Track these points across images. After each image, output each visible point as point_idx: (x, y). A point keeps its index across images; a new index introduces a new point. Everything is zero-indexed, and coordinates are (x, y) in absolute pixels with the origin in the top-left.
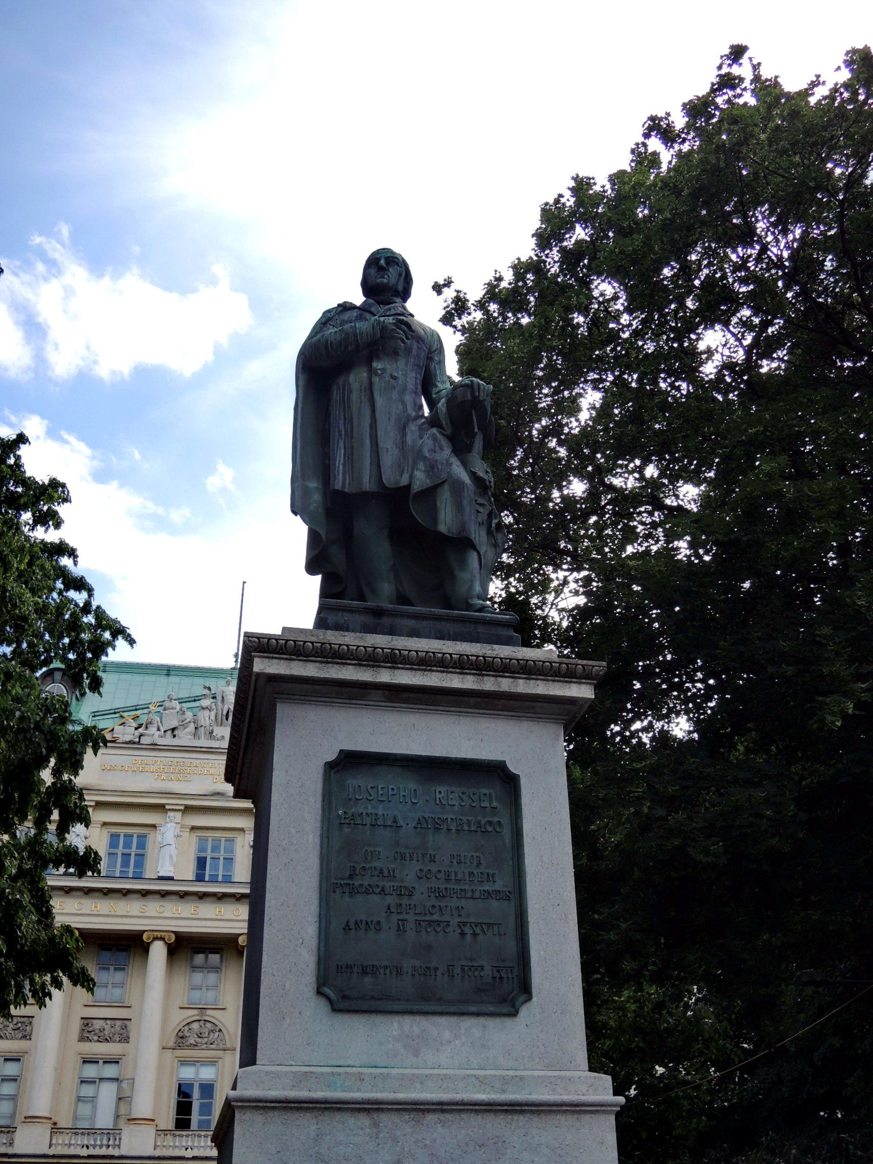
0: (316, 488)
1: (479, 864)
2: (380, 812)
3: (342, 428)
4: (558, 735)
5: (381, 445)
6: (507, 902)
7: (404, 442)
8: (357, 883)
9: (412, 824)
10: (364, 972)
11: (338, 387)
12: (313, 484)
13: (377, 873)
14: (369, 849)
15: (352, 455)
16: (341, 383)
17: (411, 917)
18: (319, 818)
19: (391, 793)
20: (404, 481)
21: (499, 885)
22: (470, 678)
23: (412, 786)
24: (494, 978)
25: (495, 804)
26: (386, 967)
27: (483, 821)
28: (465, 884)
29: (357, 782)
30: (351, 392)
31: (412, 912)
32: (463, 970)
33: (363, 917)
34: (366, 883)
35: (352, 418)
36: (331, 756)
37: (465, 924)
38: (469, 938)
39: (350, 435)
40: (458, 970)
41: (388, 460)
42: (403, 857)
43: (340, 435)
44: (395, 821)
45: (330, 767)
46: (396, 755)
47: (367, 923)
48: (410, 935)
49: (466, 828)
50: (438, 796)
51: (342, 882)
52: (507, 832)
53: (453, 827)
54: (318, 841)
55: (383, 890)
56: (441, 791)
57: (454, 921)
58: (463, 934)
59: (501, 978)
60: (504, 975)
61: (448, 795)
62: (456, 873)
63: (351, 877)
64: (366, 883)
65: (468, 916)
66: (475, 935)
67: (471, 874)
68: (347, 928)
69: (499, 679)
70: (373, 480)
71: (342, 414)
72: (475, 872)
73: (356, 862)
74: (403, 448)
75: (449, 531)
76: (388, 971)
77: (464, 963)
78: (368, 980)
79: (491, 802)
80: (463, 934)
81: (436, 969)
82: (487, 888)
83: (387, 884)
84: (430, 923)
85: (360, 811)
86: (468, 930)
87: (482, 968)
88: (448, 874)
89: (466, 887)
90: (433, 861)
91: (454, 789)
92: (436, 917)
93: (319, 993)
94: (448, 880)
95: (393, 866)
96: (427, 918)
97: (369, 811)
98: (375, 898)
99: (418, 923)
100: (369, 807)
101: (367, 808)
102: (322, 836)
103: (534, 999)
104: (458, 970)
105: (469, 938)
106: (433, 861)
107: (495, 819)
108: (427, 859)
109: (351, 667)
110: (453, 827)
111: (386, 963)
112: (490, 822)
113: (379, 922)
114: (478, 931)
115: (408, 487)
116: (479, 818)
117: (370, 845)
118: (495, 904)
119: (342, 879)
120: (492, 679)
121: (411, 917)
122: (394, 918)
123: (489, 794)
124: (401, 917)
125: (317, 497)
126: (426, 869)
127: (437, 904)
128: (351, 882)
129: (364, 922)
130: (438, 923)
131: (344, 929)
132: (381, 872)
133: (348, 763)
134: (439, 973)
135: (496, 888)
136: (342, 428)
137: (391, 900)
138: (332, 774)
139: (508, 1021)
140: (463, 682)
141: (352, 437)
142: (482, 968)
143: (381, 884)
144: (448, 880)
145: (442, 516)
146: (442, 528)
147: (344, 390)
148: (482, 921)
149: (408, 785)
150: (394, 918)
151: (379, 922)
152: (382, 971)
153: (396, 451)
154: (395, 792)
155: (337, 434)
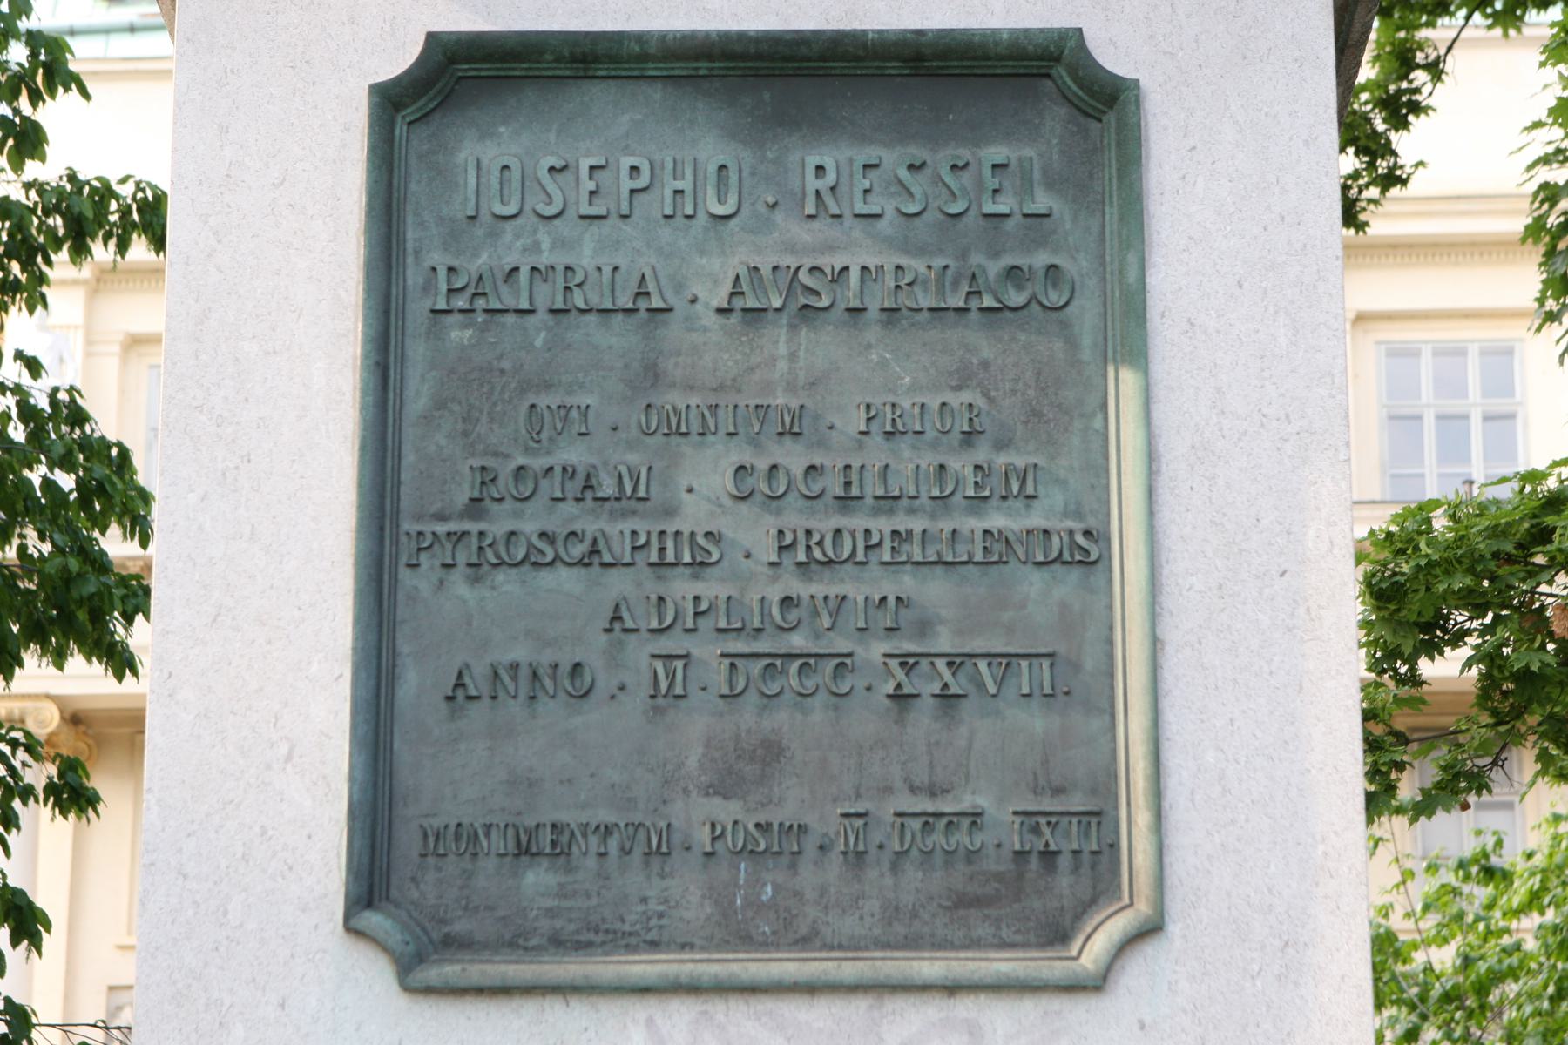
2: (585, 258)
6: (1075, 574)
8: (497, 529)
10: (524, 850)
13: (574, 487)
14: (543, 401)
17: (707, 650)
19: (627, 184)
23: (712, 150)
25: (1042, 201)
26: (607, 830)
27: (994, 268)
28: (911, 511)
29: (490, 152)
31: (705, 624)
33: (520, 653)
34: (530, 527)
37: (908, 663)
46: (640, 37)
47: (535, 675)
51: (441, 528)
55: (594, 551)
56: (823, 160)
63: (475, 508)
64: (530, 527)
68: (458, 694)
73: (496, 454)
76: (613, 844)
78: (537, 879)
82: (997, 520)
84: (775, 663)
85: (509, 261)
91: (871, 153)
93: (351, 929)
94: (846, 502)
95: (633, 458)
97: (544, 260)
98: (565, 579)
100: (546, 244)
101: (535, 247)
107: (1041, 259)
111: (605, 816)
112: (1013, 273)
116: (976, 259)
117: (548, 386)
118: (1033, 583)
119: (441, 517)
121: (707, 650)
123: (1010, 160)
124: (666, 645)
126: (763, 465)
128: (473, 527)
129: (524, 673)
131: (450, 699)
138: (400, 129)
142: (975, 818)
143: (590, 526)
148: (978, 645)
149: (698, 146)
150: (639, 652)
152: (594, 840)
154: (643, 181)
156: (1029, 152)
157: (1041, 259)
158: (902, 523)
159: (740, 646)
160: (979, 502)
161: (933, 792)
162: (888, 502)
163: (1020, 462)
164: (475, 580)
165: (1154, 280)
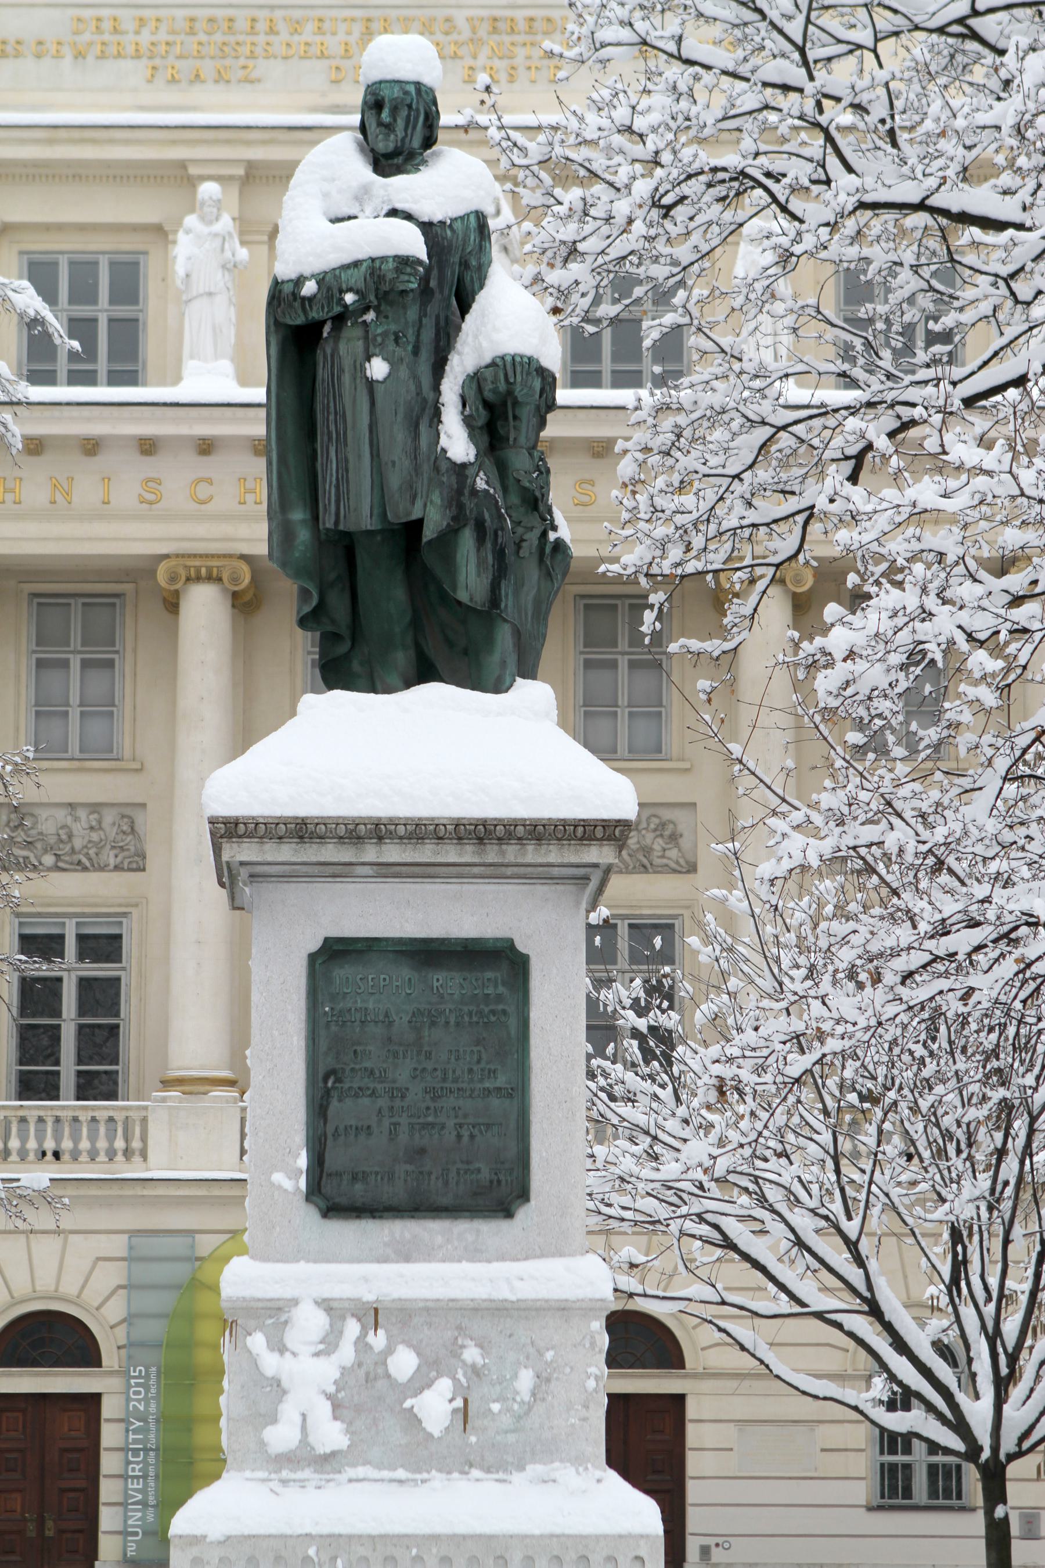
0: (304, 521)
1: (479, 1062)
2: (371, 1006)
3: (332, 428)
4: (578, 903)
5: (385, 457)
7: (416, 449)
8: (346, 1086)
9: (406, 1018)
10: (355, 1178)
11: (325, 357)
12: (298, 515)
15: (347, 471)
16: (329, 351)
17: (404, 1120)
18: (303, 1017)
20: (416, 515)
21: (501, 1081)
22: (469, 848)
24: (491, 1182)
26: (377, 1173)
27: (486, 1010)
29: (343, 972)
30: (342, 370)
32: (458, 1173)
33: (353, 1123)
36: (315, 945)
37: (461, 1126)
38: (466, 1139)
39: (342, 441)
40: (453, 1174)
41: (395, 480)
42: (396, 1055)
43: (330, 439)
44: (387, 1015)
45: (312, 958)
48: (403, 1137)
49: (466, 1019)
50: (435, 984)
52: (513, 1022)
53: (452, 1021)
54: (303, 1043)
57: (451, 1123)
58: (459, 1137)
59: (499, 1182)
60: (502, 1177)
61: (448, 982)
62: (454, 1072)
64: (355, 1085)
65: (465, 1116)
66: (472, 1137)
67: (470, 1071)
69: (504, 847)
70: (375, 512)
71: (332, 405)
72: (475, 1068)
75: (471, 600)
77: (460, 1165)
78: (359, 1187)
79: (496, 987)
80: (459, 1137)
81: (430, 1173)
82: (487, 1085)
83: (379, 1086)
84: (426, 1126)
85: (349, 1005)
86: (465, 1133)
87: (479, 1170)
88: (445, 1072)
89: (464, 1085)
90: (428, 1056)
91: (454, 974)
92: (430, 1119)
96: (421, 1120)
97: (359, 1005)
98: (366, 1101)
99: (412, 1126)
102: (307, 1038)
103: (533, 1202)
104: (453, 1174)
105: (466, 1139)
106: (428, 1056)
107: (500, 1007)
108: (422, 1057)
109: (330, 846)
110: (452, 1021)
111: (377, 1169)
112: (493, 1012)
113: (369, 1127)
114: (476, 1132)
115: (419, 523)
117: (359, 1044)
118: (495, 1102)
120: (496, 847)
121: (404, 1120)
122: (386, 1122)
123: (492, 980)
124: (393, 1120)
125: (303, 535)
127: (432, 1105)
130: (432, 1125)
132: (372, 1072)
133: (334, 954)
134: (433, 1177)
135: (498, 1084)
136: (332, 428)
137: (382, 1102)
139: (504, 1225)
141: (346, 445)
142: (479, 1170)
143: (372, 1086)
144: (444, 1080)
145: (462, 578)
146: (463, 596)
147: (332, 366)
148: (481, 1121)
150: (386, 1122)
151: (369, 1127)
153: (407, 463)
155: (326, 438)
156: (498, 975)
157: (500, 1007)
158: (460, 1085)
159: (415, 1120)
160: (481, 1081)
161: (468, 1163)
162: (456, 1080)
163: (493, 1068)
164: (340, 1101)
165: (532, 1015)
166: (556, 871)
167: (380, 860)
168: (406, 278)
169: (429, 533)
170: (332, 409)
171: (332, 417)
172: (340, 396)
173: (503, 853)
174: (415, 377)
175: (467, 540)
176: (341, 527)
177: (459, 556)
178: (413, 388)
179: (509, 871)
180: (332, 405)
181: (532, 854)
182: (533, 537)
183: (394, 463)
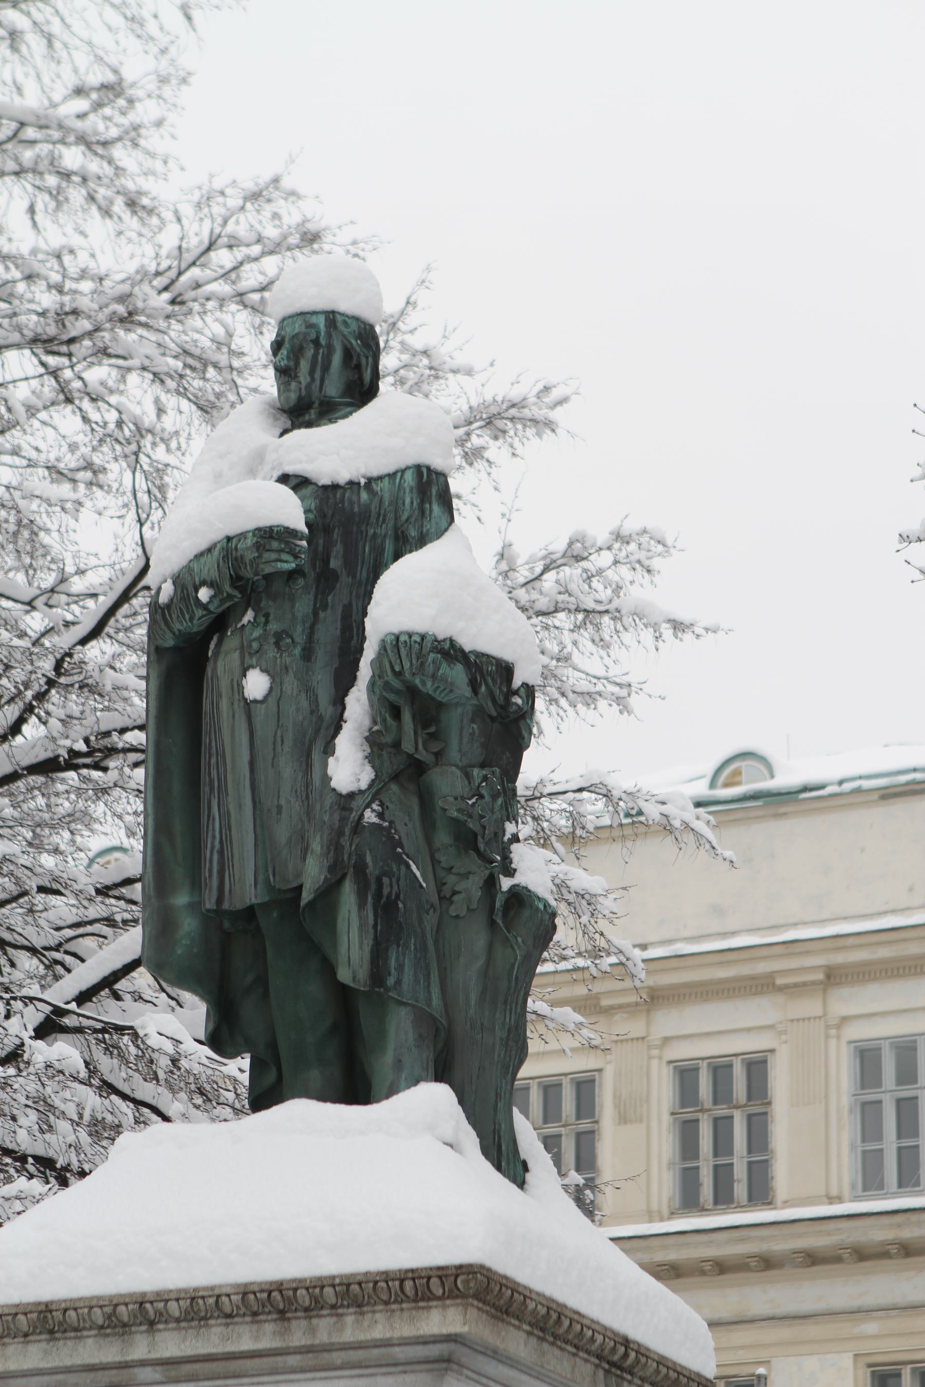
7: (308, 784)
22: (269, 1328)
35: (224, 750)
39: (223, 790)
41: (282, 832)
69: (315, 1321)
74: (307, 797)
75: (354, 978)
109: (90, 1341)
120: (304, 1323)
125: (188, 925)
140: (257, 1339)
141: (227, 794)
145: (343, 949)
153: (297, 806)
155: (207, 789)
166: (399, 1353)
167: (154, 1355)
168: (273, 556)
169: (306, 896)
170: (214, 751)
171: (213, 760)
172: (220, 729)
173: (313, 1331)
174: (309, 691)
175: (348, 894)
176: (226, 906)
177: (340, 920)
178: (305, 704)
179: (338, 1357)
180: (213, 744)
181: (351, 1329)
182: (473, 886)
183: (279, 808)
